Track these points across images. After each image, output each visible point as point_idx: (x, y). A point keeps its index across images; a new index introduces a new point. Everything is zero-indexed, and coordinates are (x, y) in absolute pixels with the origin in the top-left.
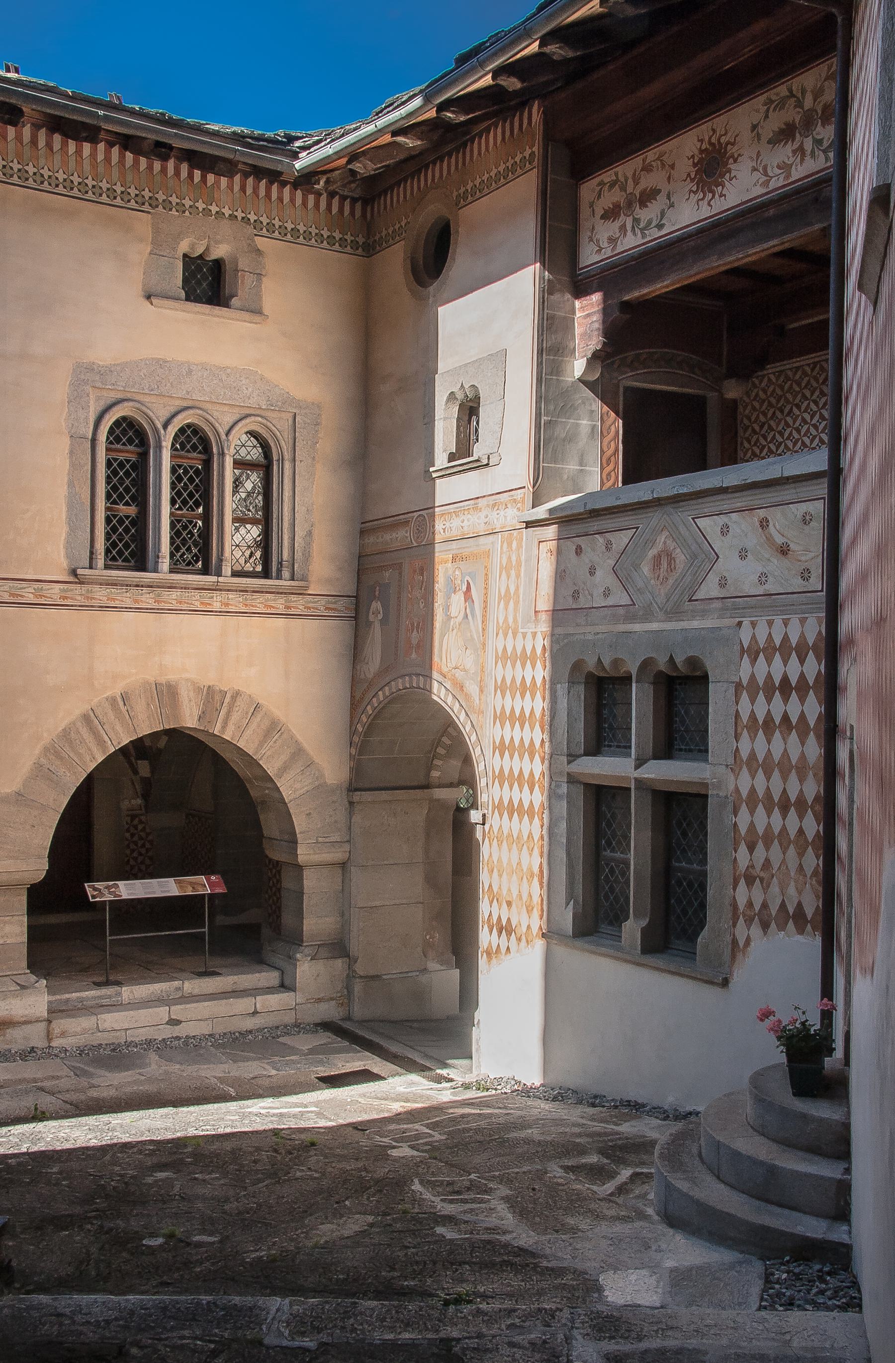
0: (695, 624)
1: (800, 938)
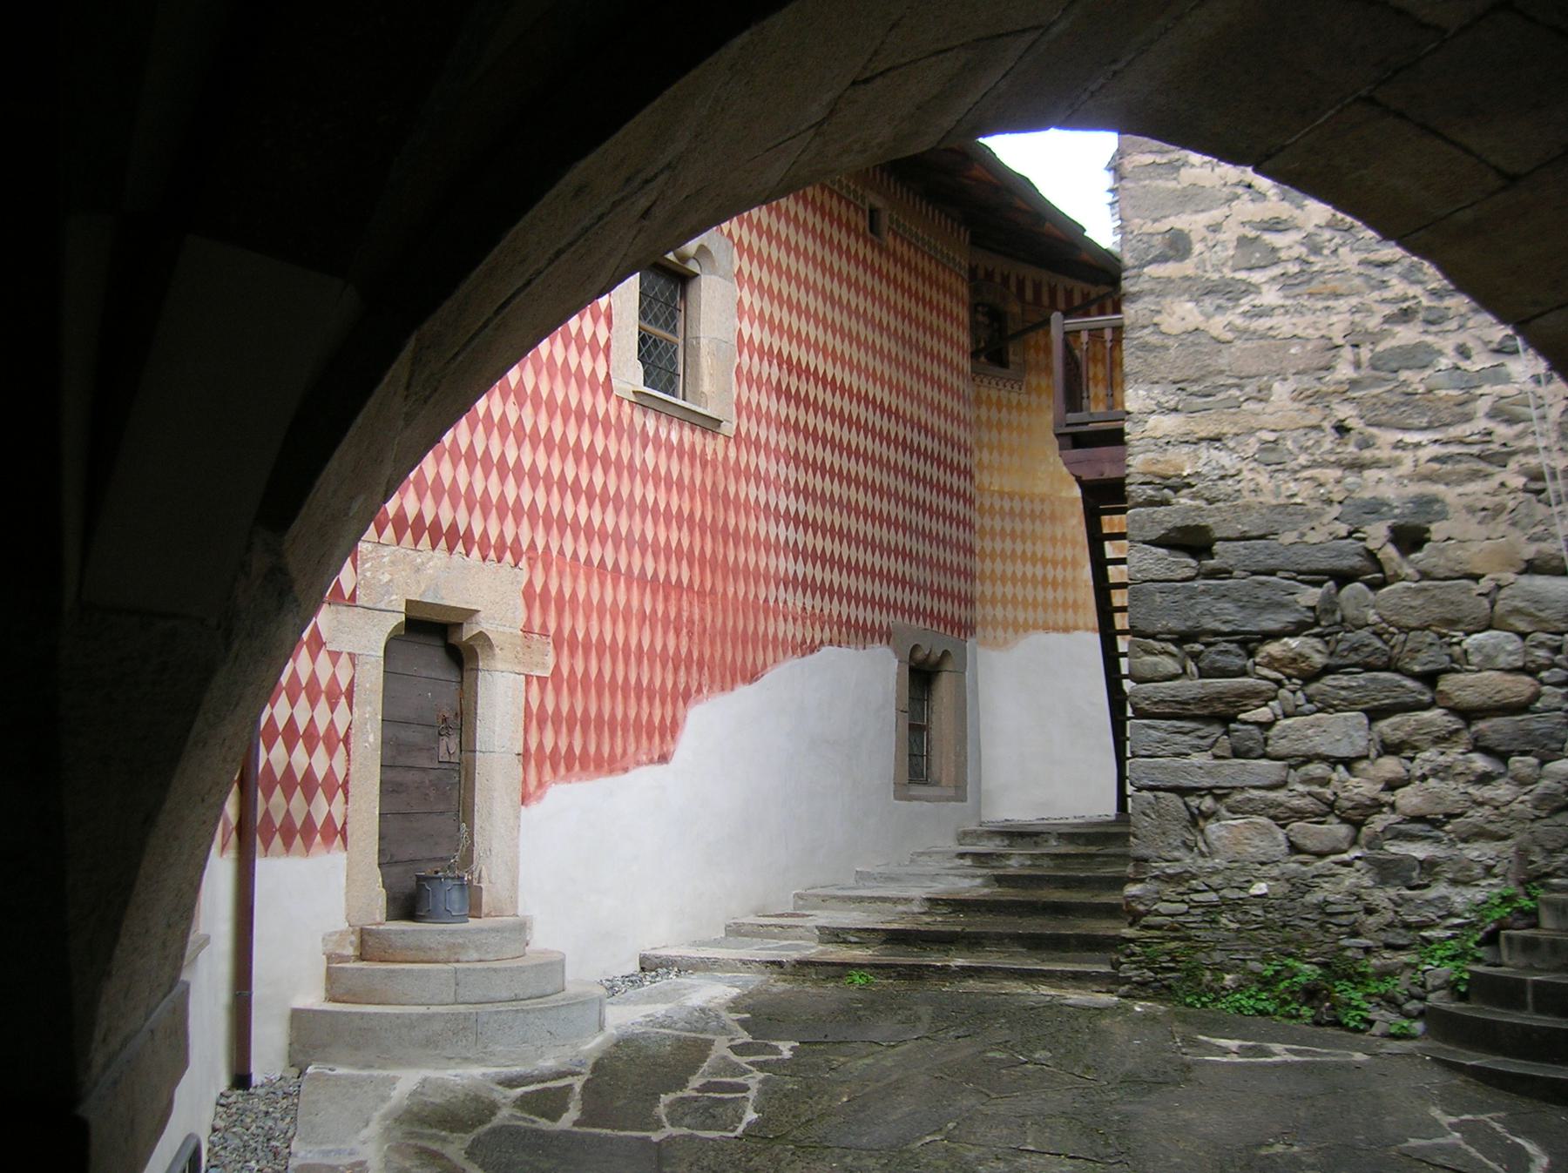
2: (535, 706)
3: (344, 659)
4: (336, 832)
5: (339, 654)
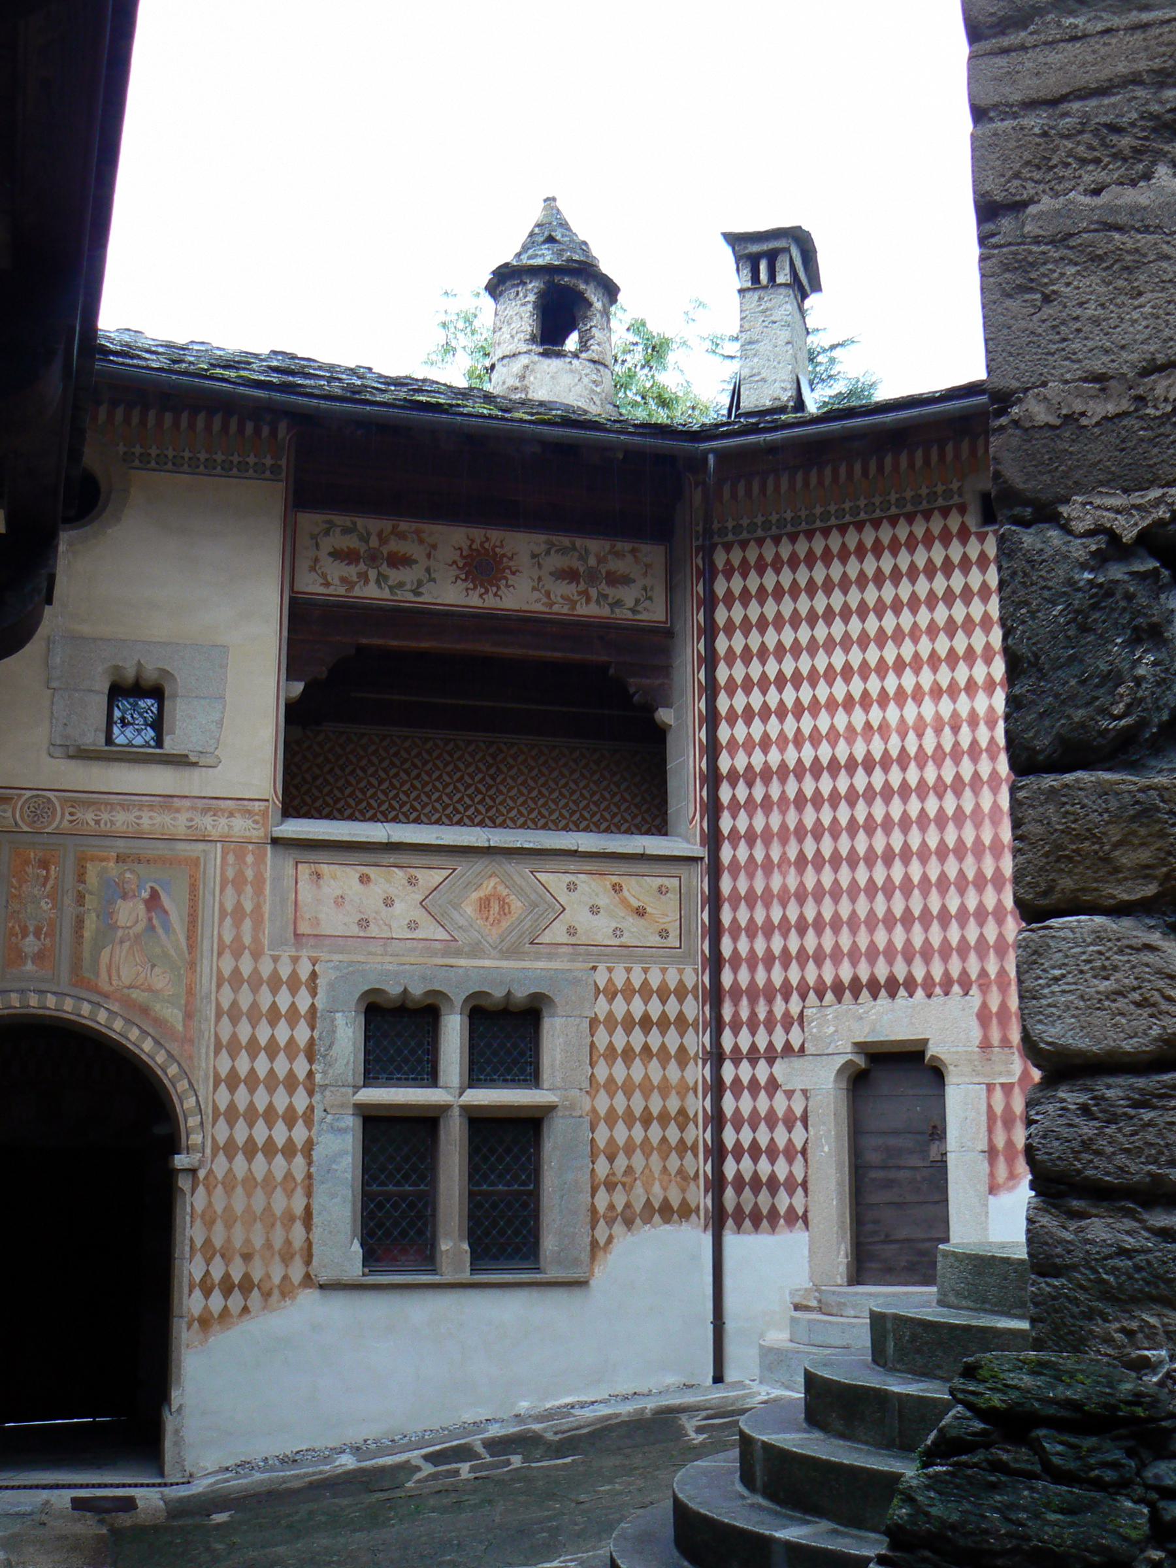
0: (540, 964)
1: (667, 1227)
2: (999, 1109)
3: (798, 1095)
4: (797, 1218)
5: (793, 1091)
